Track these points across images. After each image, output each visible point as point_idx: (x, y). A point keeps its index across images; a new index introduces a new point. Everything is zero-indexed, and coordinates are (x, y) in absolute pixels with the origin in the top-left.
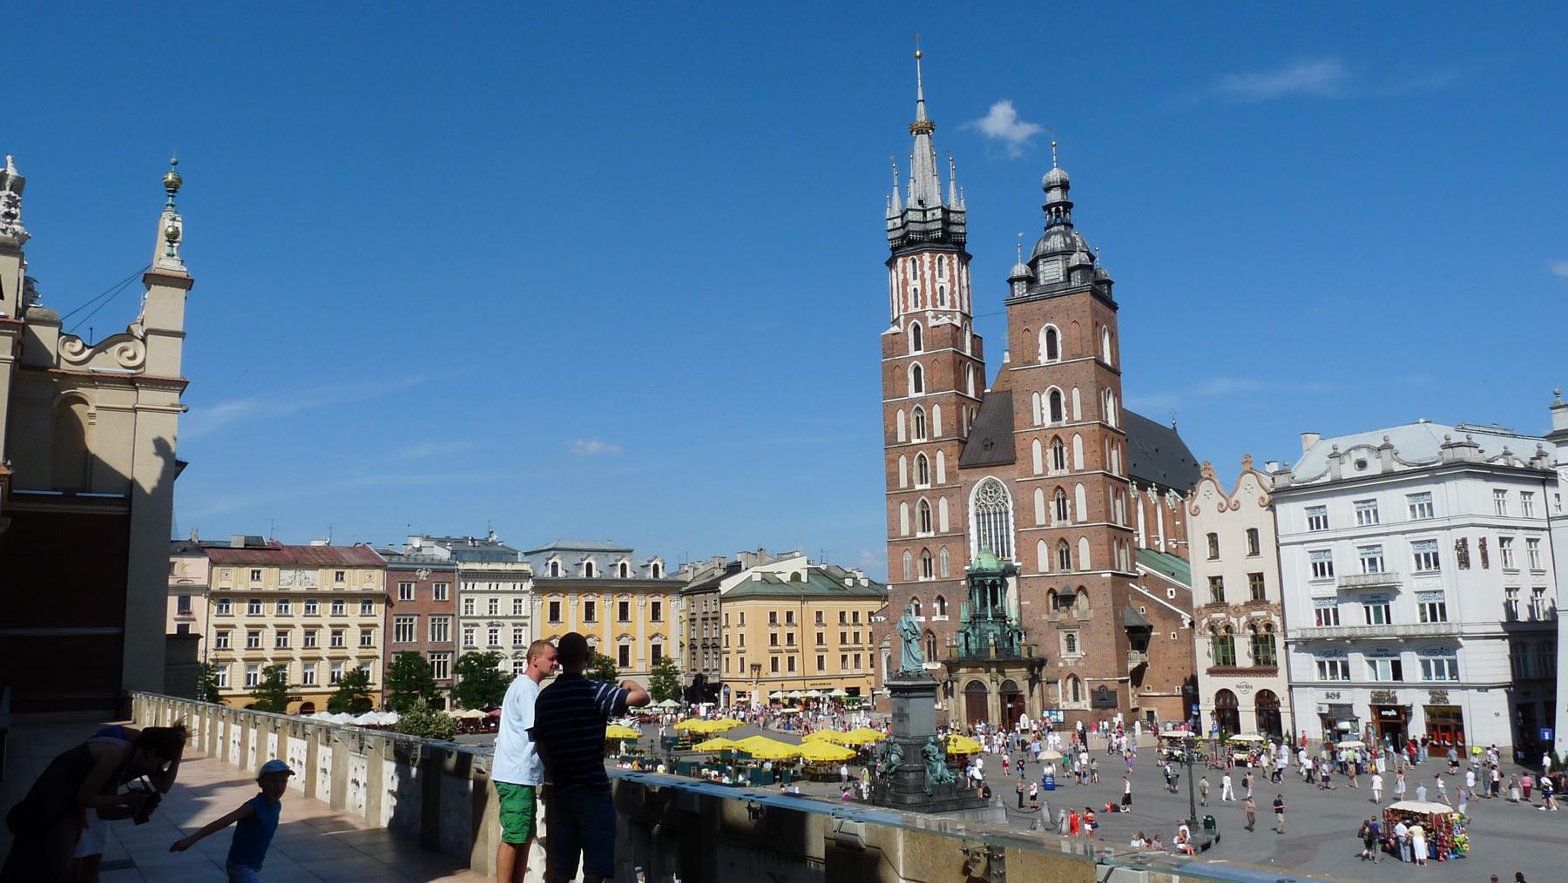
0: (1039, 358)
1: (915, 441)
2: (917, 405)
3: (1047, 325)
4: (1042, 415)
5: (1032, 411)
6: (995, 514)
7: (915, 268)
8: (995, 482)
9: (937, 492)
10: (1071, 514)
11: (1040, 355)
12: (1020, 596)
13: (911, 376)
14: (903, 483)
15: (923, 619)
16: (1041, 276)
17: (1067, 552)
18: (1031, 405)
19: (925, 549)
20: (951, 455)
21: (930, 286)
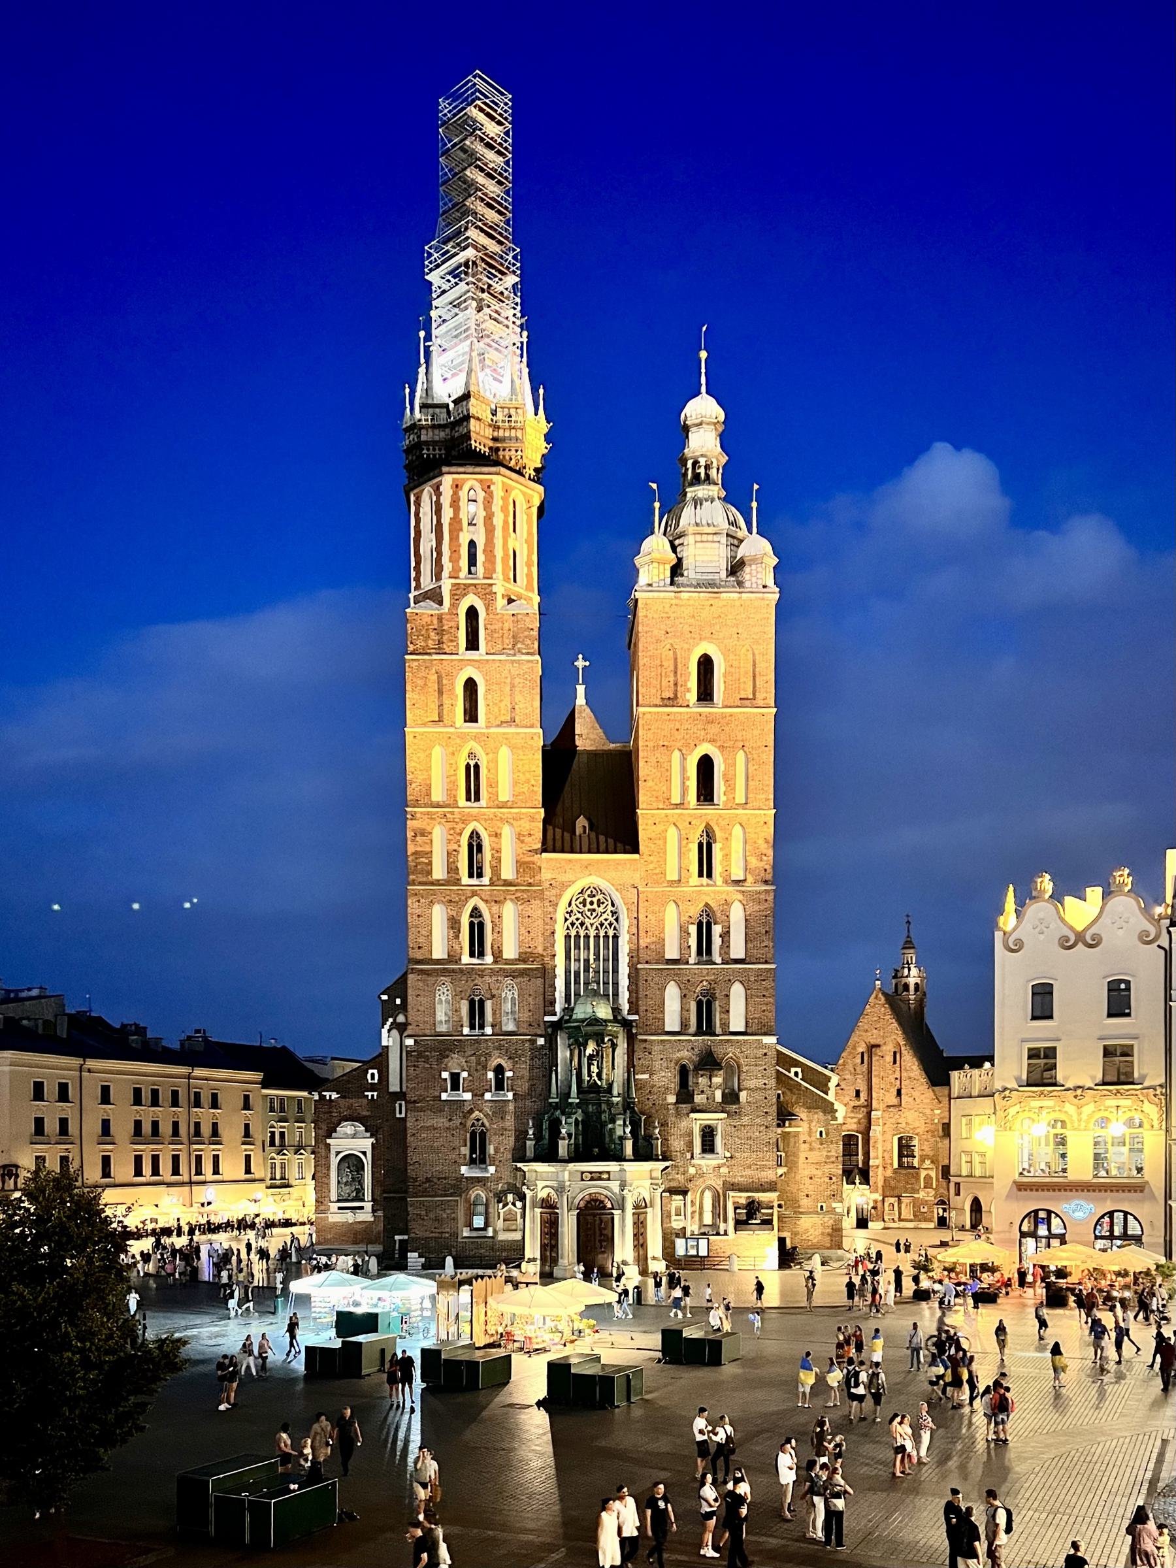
0: (688, 696)
5: (669, 780)
6: (597, 937)
10: (721, 948)
11: (689, 690)
12: (634, 1067)
15: (468, 1096)
18: (669, 770)
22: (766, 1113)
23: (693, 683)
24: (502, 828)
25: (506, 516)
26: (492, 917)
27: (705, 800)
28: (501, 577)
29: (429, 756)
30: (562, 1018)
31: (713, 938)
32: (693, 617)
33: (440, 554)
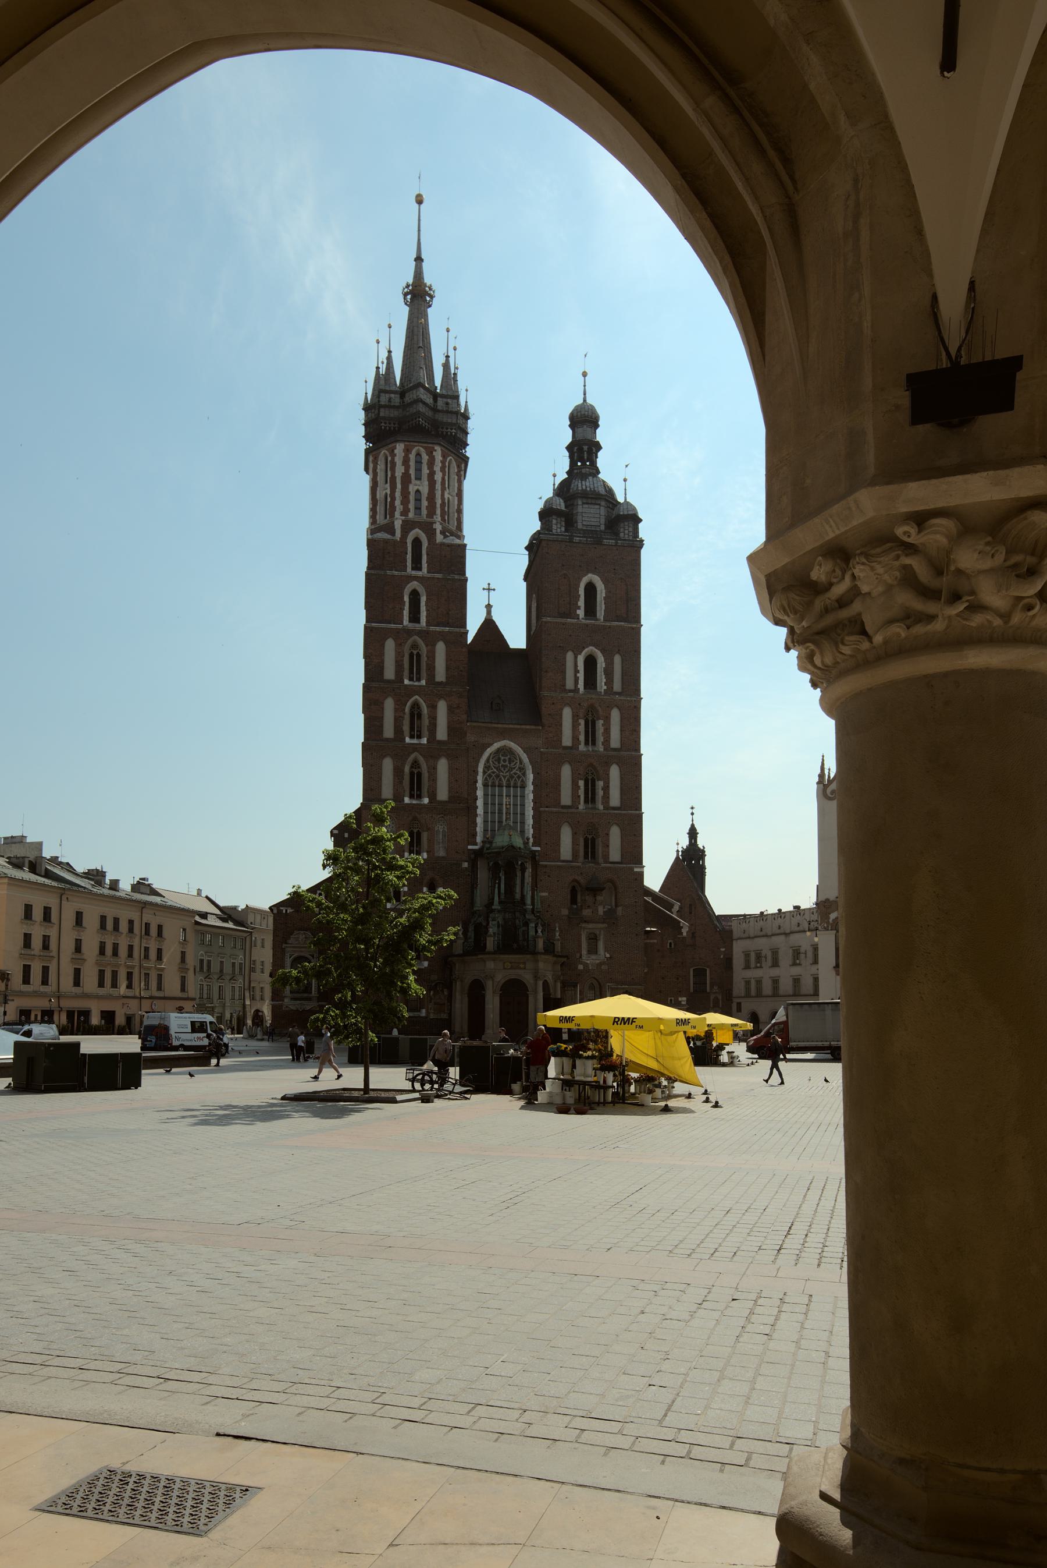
0: (578, 612)
1: (406, 682)
2: (416, 637)
3: (590, 575)
4: (576, 679)
5: (564, 672)
7: (419, 462)
8: (510, 751)
9: (434, 751)
10: (603, 797)
11: (579, 608)
13: (406, 599)
14: (389, 732)
16: (579, 518)
17: (593, 840)
18: (564, 665)
19: (415, 819)
20: (458, 707)
21: (440, 492)
22: (637, 924)
23: (581, 603)
24: (437, 702)
25: (444, 475)
26: (428, 768)
27: (591, 689)
28: (439, 519)
29: (383, 646)
30: (482, 849)
31: (597, 791)
32: (582, 555)
33: (393, 499)
